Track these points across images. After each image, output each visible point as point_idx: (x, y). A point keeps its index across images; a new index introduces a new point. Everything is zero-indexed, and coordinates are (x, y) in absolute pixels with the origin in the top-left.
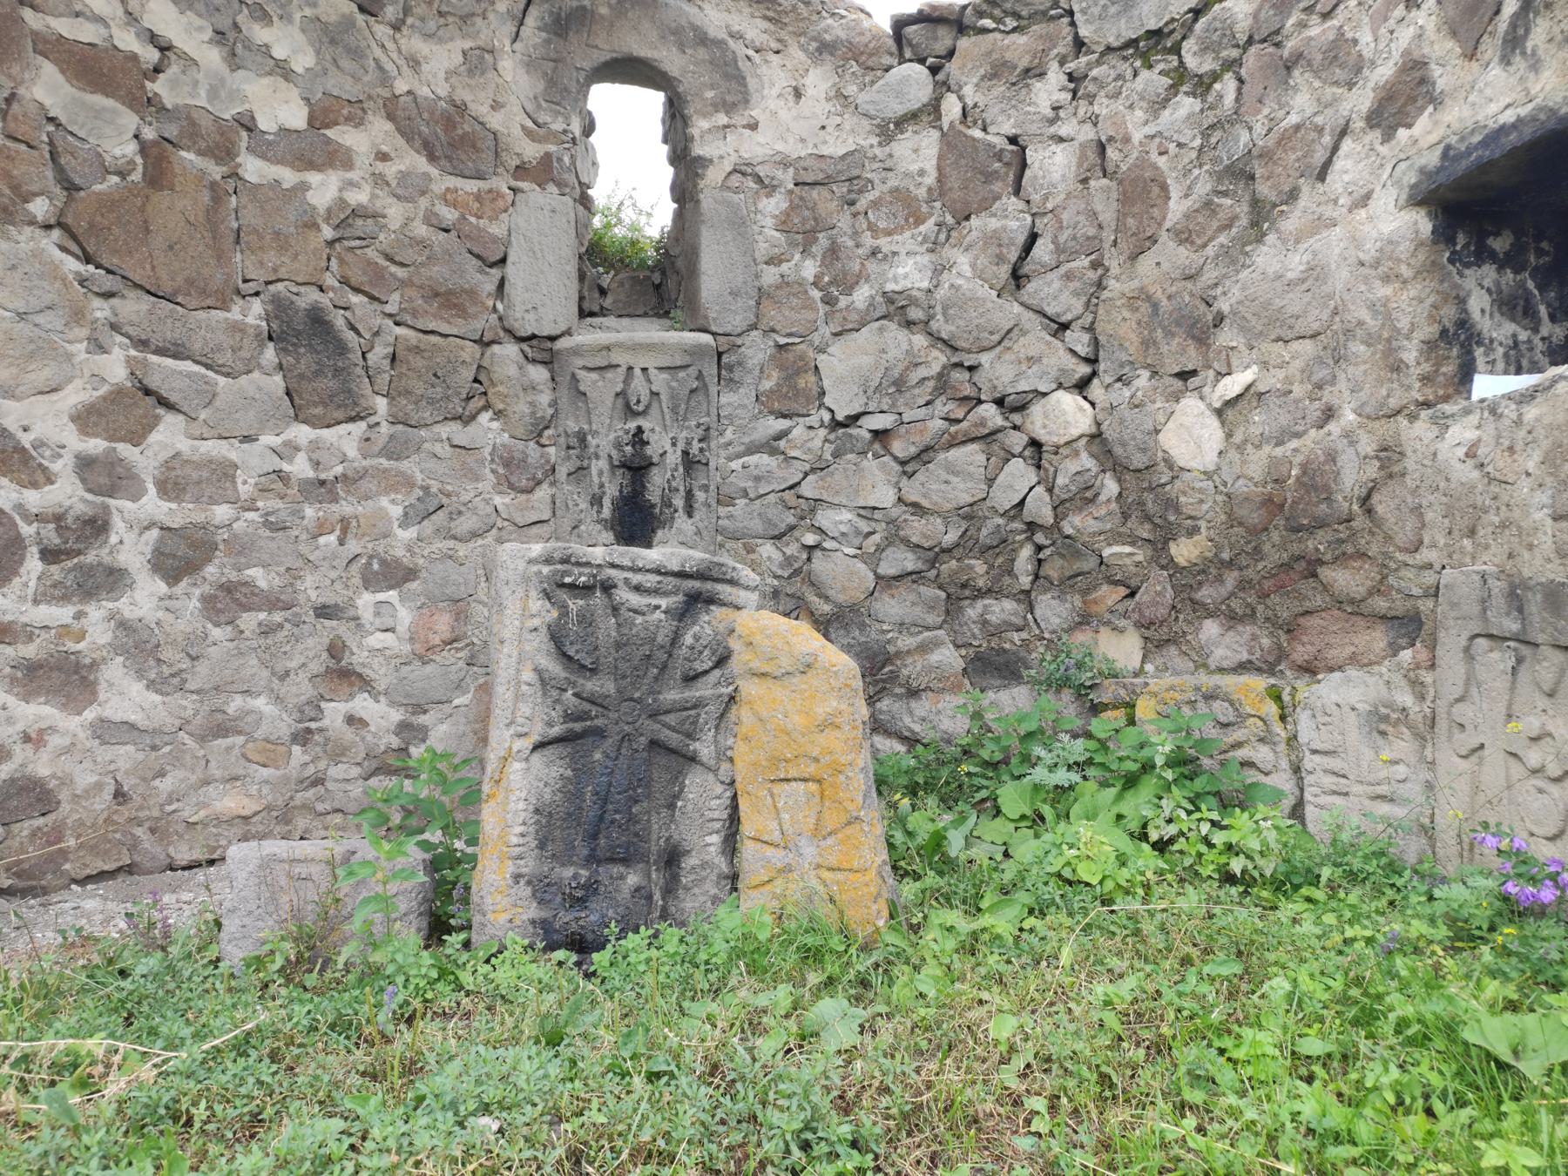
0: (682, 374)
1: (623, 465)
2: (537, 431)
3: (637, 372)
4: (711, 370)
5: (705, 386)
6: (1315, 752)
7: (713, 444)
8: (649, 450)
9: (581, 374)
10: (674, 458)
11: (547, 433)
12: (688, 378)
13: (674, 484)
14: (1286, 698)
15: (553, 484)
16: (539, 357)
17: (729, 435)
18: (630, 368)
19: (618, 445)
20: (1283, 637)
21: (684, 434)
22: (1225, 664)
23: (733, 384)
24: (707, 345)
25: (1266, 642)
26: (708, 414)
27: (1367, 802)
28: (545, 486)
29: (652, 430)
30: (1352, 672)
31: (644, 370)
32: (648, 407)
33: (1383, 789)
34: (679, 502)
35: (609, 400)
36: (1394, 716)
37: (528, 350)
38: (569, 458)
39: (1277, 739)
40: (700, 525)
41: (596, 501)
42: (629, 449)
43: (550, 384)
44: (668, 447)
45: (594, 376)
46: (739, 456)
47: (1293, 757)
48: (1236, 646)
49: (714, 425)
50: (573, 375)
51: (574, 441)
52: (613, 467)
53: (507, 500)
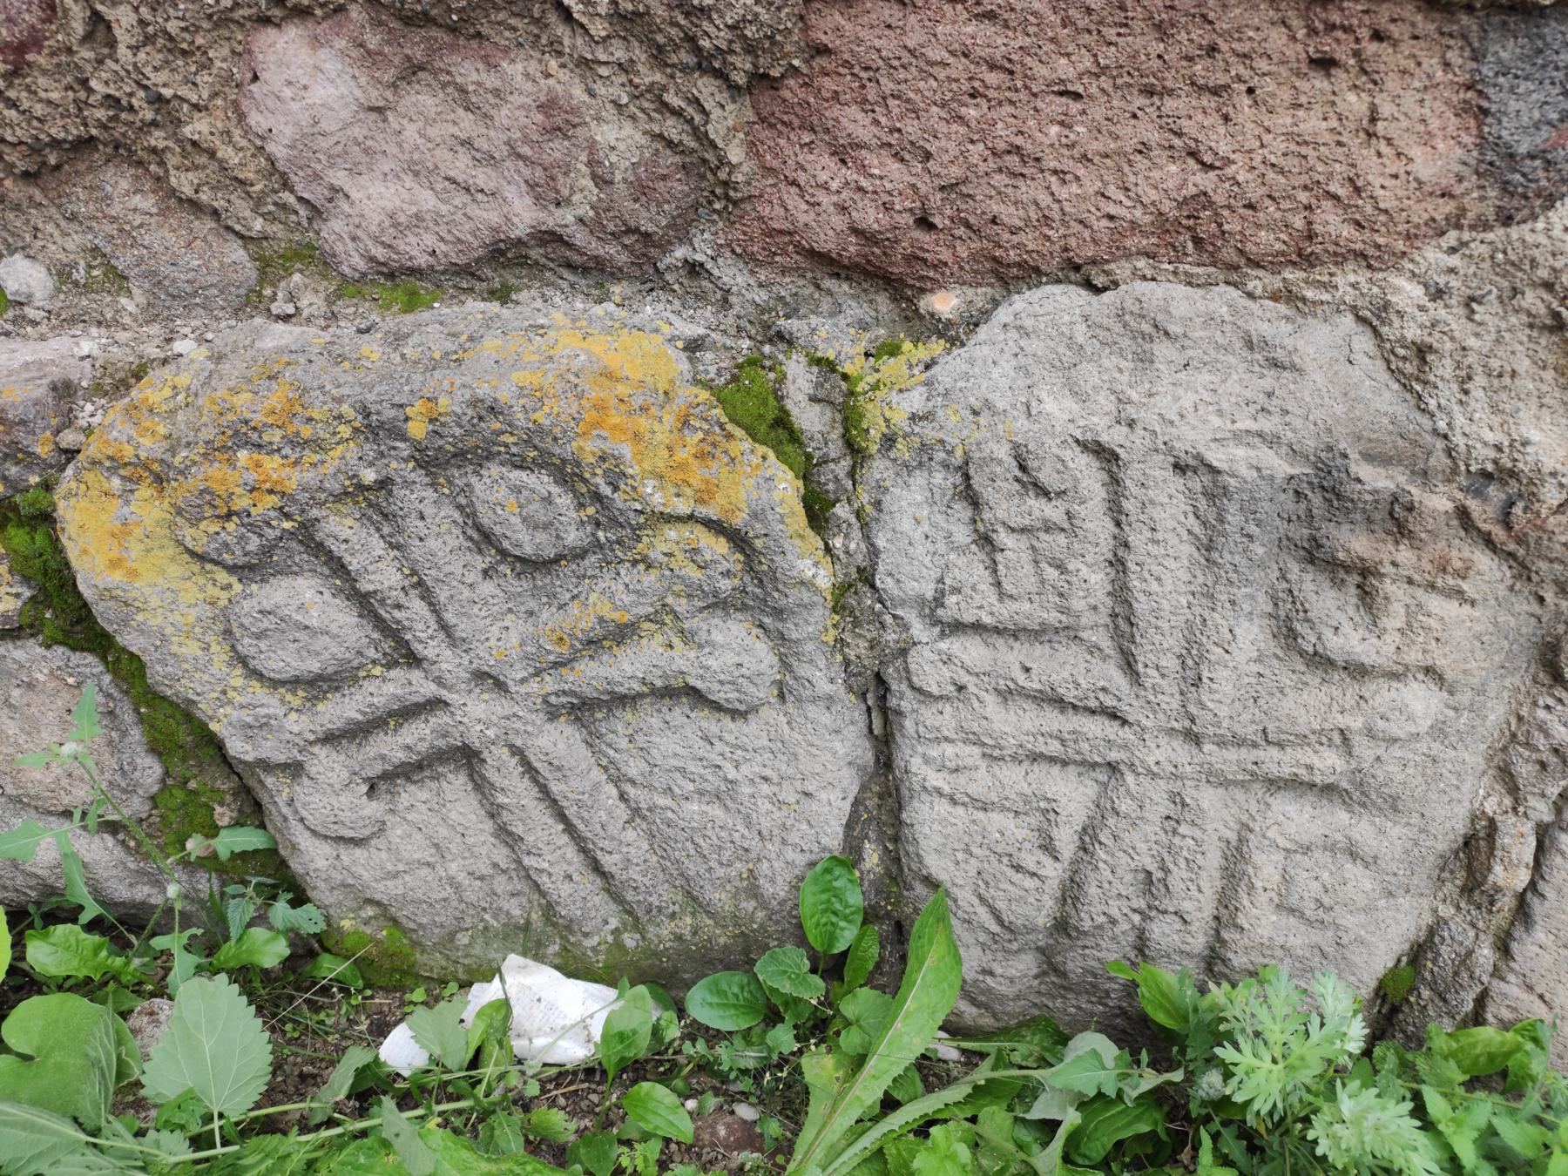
6: (957, 627)
14: (810, 419)
20: (725, 119)
22: (416, 249)
25: (621, 140)
27: (1208, 799)
30: (1173, 297)
33: (1328, 763)
36: (1439, 502)
39: (796, 595)
47: (858, 648)
48: (460, 166)
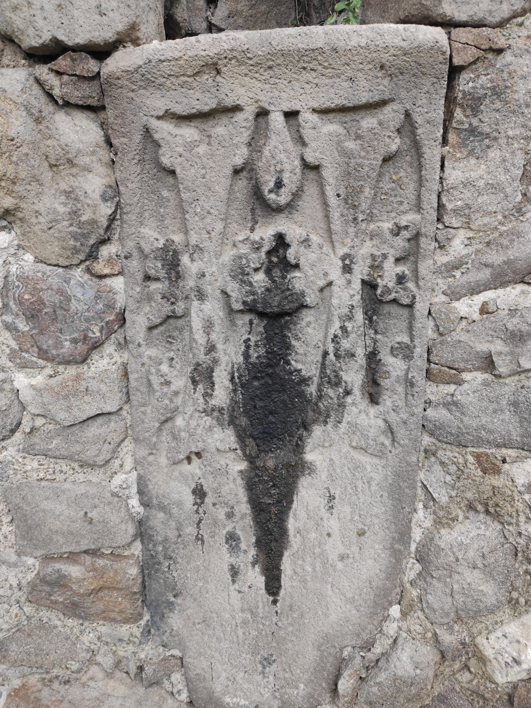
0: (368, 122)
1: (250, 308)
2: (89, 248)
3: (277, 119)
4: (430, 111)
5: (416, 145)
7: (425, 267)
8: (298, 281)
9: (164, 130)
10: (347, 294)
11: (106, 251)
12: (381, 130)
13: (346, 344)
15: (124, 345)
16: (76, 94)
17: (458, 246)
18: (262, 114)
19: (240, 273)
21: (367, 248)
23: (476, 139)
24: (434, 49)
26: (418, 208)
28: (109, 348)
29: (306, 242)
31: (291, 115)
32: (296, 195)
34: (354, 376)
35: (221, 182)
37: (52, 80)
38: (150, 298)
40: (393, 418)
41: (202, 376)
42: (260, 279)
43: (105, 154)
44: (335, 274)
45: (189, 132)
46: (474, 290)
49: (429, 229)
50: (147, 131)
51: (156, 267)
52: (231, 311)
53: (39, 380)
